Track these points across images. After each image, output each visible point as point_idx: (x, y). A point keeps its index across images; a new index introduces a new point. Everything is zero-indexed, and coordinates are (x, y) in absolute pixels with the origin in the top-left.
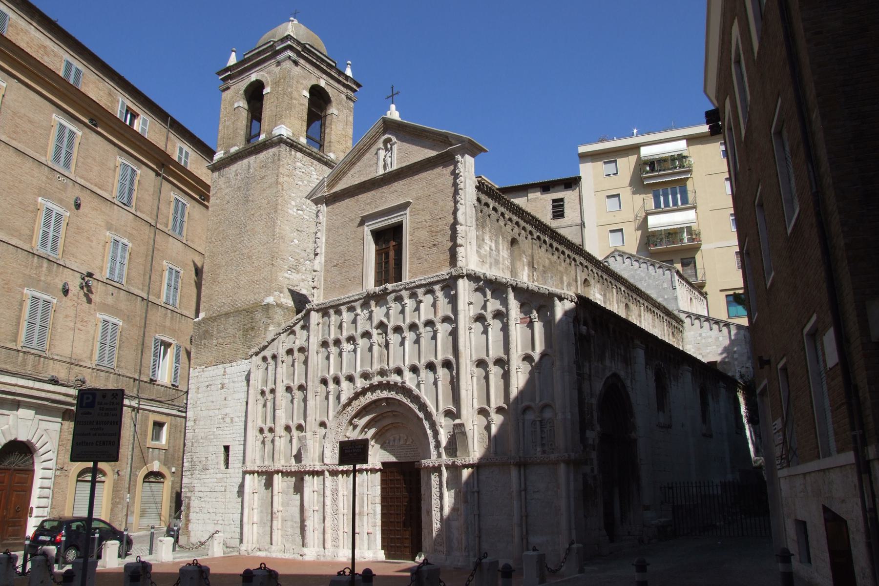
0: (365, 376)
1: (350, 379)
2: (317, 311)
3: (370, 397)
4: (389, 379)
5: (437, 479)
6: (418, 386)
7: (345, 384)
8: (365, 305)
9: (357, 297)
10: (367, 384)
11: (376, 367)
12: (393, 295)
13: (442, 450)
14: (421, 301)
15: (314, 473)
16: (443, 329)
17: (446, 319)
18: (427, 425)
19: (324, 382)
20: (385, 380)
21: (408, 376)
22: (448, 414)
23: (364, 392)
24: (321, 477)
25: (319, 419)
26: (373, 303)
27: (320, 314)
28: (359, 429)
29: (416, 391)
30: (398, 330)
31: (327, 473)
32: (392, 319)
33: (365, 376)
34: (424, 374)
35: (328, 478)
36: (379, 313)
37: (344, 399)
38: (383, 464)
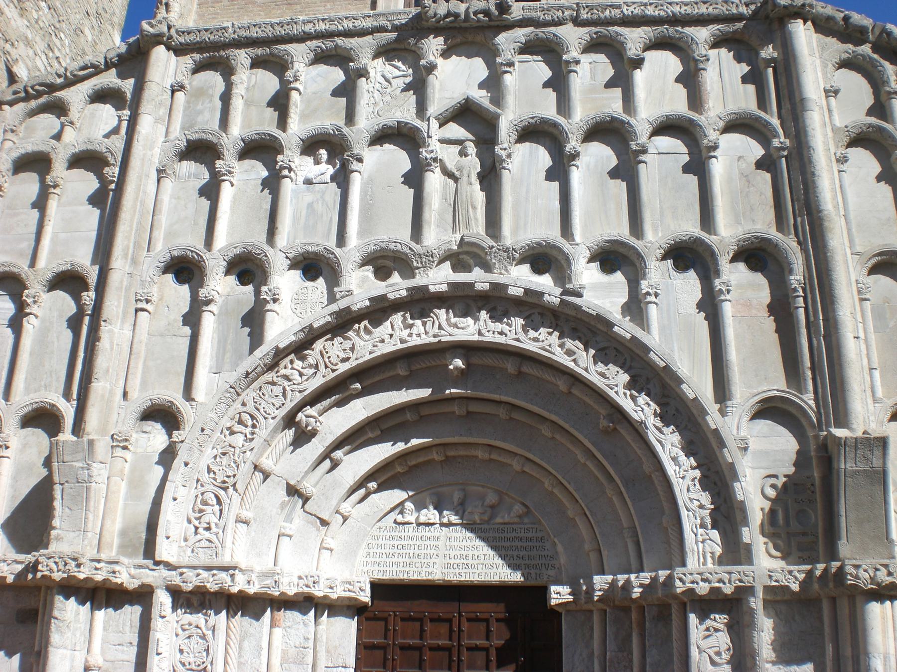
0: (383, 262)
1: (312, 266)
2: (179, 51)
3: (396, 335)
4: (496, 277)
5: (723, 640)
6: (635, 307)
7: (285, 282)
8: (402, 44)
9: (368, 24)
10: (397, 286)
11: (438, 236)
12: (521, 34)
13: (752, 534)
14: (638, 63)
15: (103, 595)
16: (733, 155)
17: (738, 124)
18: (668, 444)
19: (185, 269)
20: (479, 278)
21: (587, 275)
22: (770, 409)
23: (379, 311)
24: (132, 613)
25: (140, 399)
26: (433, 45)
27: (188, 61)
28: (316, 447)
29: (625, 328)
30: (535, 132)
31: (163, 599)
32: (510, 100)
33: (383, 262)
34: (658, 274)
35: (168, 623)
36: (457, 77)
37: (280, 328)
38: (379, 588)
